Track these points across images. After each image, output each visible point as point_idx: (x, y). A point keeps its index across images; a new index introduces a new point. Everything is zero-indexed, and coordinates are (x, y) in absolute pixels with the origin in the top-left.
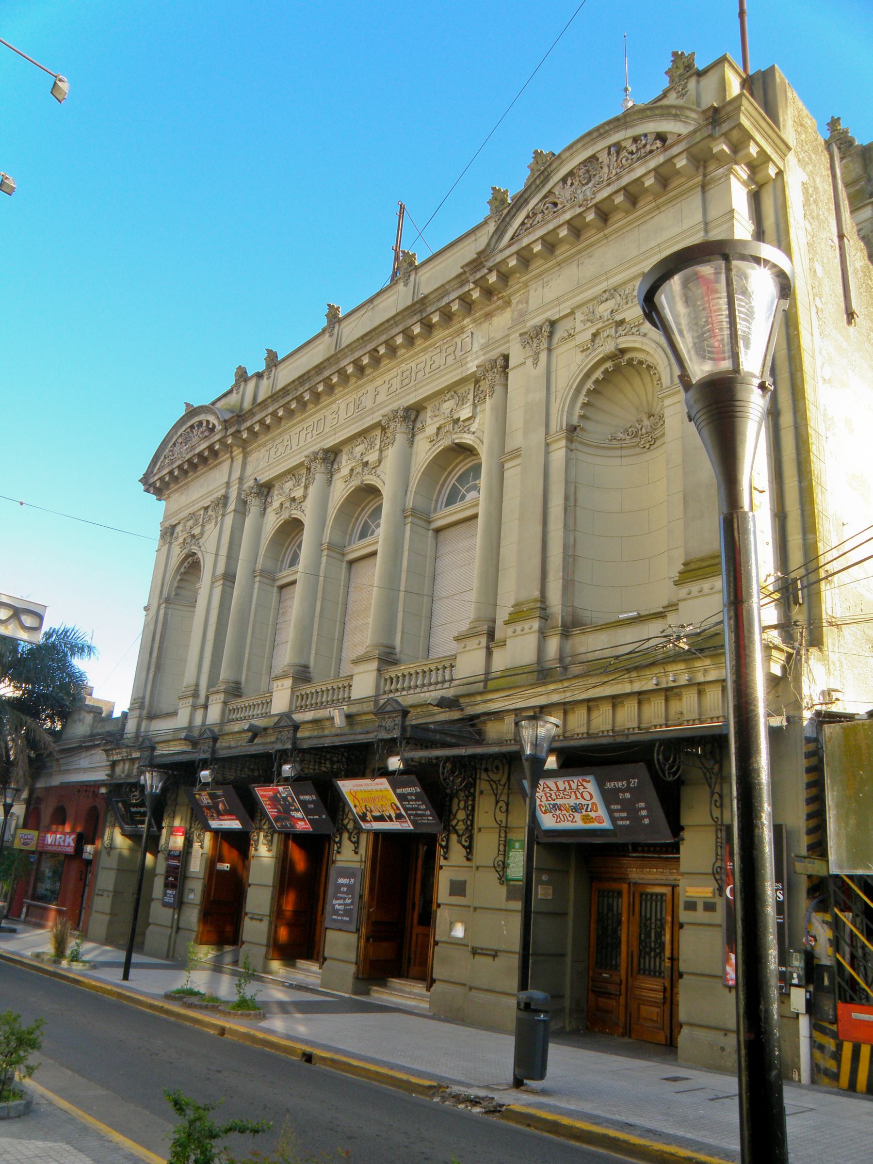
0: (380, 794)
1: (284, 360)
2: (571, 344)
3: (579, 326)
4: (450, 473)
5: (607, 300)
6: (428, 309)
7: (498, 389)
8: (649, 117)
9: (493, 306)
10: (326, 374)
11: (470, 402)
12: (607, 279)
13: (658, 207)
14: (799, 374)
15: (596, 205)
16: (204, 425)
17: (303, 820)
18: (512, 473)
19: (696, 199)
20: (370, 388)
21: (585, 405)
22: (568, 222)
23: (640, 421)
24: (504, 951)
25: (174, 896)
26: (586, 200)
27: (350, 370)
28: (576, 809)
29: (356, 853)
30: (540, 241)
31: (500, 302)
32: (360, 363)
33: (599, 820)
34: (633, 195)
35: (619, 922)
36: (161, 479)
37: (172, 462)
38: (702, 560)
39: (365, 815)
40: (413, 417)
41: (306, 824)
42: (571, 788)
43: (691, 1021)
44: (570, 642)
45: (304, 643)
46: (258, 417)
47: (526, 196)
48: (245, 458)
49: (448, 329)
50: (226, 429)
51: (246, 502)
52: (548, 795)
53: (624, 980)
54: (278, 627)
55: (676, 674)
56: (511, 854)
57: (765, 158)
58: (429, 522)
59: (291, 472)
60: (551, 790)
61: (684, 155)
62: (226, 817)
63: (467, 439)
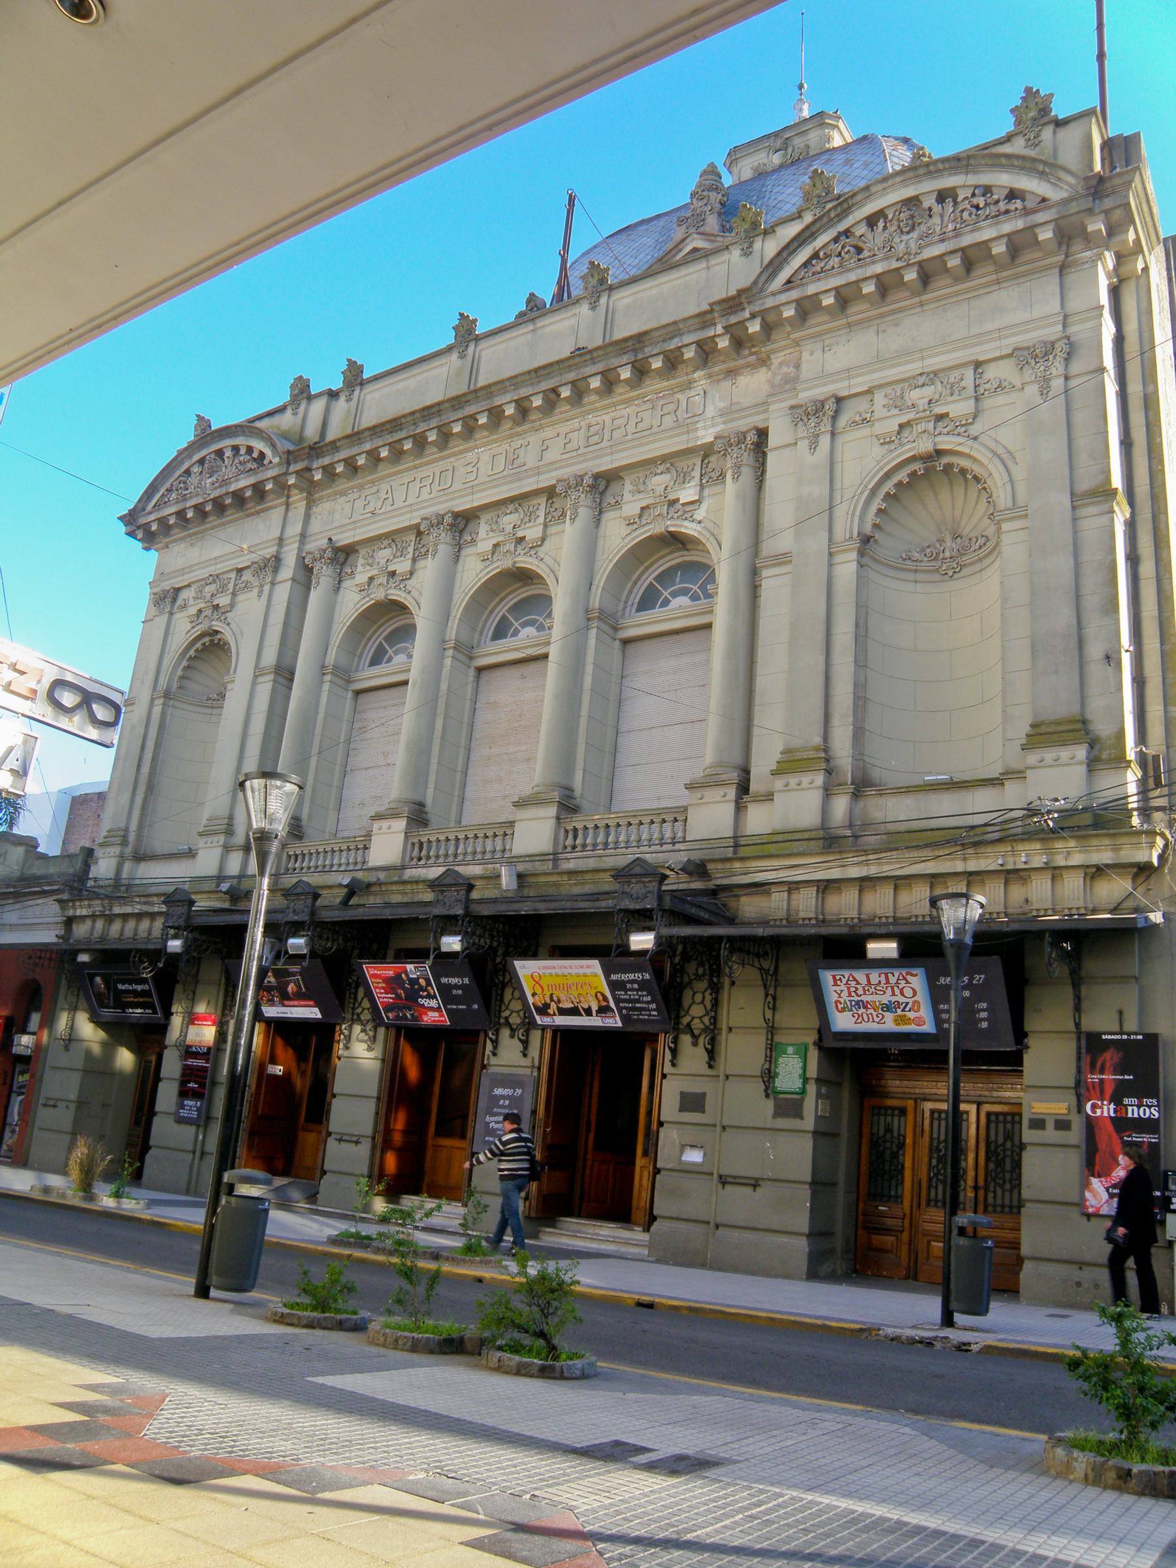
0: (582, 980)
2: (866, 431)
3: (879, 412)
4: (647, 568)
5: (923, 385)
6: (646, 350)
7: (747, 474)
8: (1001, 165)
9: (742, 362)
10: (470, 410)
11: (696, 481)
12: (922, 358)
13: (998, 282)
14: (1162, 517)
15: (920, 263)
16: (243, 451)
17: (438, 1009)
18: (773, 584)
19: (1051, 284)
20: (534, 439)
21: (880, 511)
22: (878, 277)
23: (941, 541)
24: (769, 1180)
25: (199, 1110)
26: (909, 254)
27: (510, 410)
28: (888, 1008)
29: (525, 1055)
30: (833, 293)
31: (753, 358)
32: (526, 403)
33: (919, 1021)
34: (972, 259)
35: (902, 1145)
36: (162, 521)
37: (185, 498)
38: (1058, 723)
39: (547, 1006)
40: (602, 488)
41: (155, 1012)
42: (887, 981)
43: (1038, 1255)
44: (861, 804)
45: (418, 771)
46: (343, 454)
47: (814, 229)
48: (309, 508)
49: (668, 380)
50: (289, 464)
51: (310, 570)
52: (852, 989)
53: (908, 1213)
54: (352, 746)
55: (1030, 855)
56: (781, 1060)
57: (1138, 249)
58: (616, 629)
59: (391, 537)
60: (858, 983)
61: (1051, 226)
62: (296, 1003)
63: (689, 528)
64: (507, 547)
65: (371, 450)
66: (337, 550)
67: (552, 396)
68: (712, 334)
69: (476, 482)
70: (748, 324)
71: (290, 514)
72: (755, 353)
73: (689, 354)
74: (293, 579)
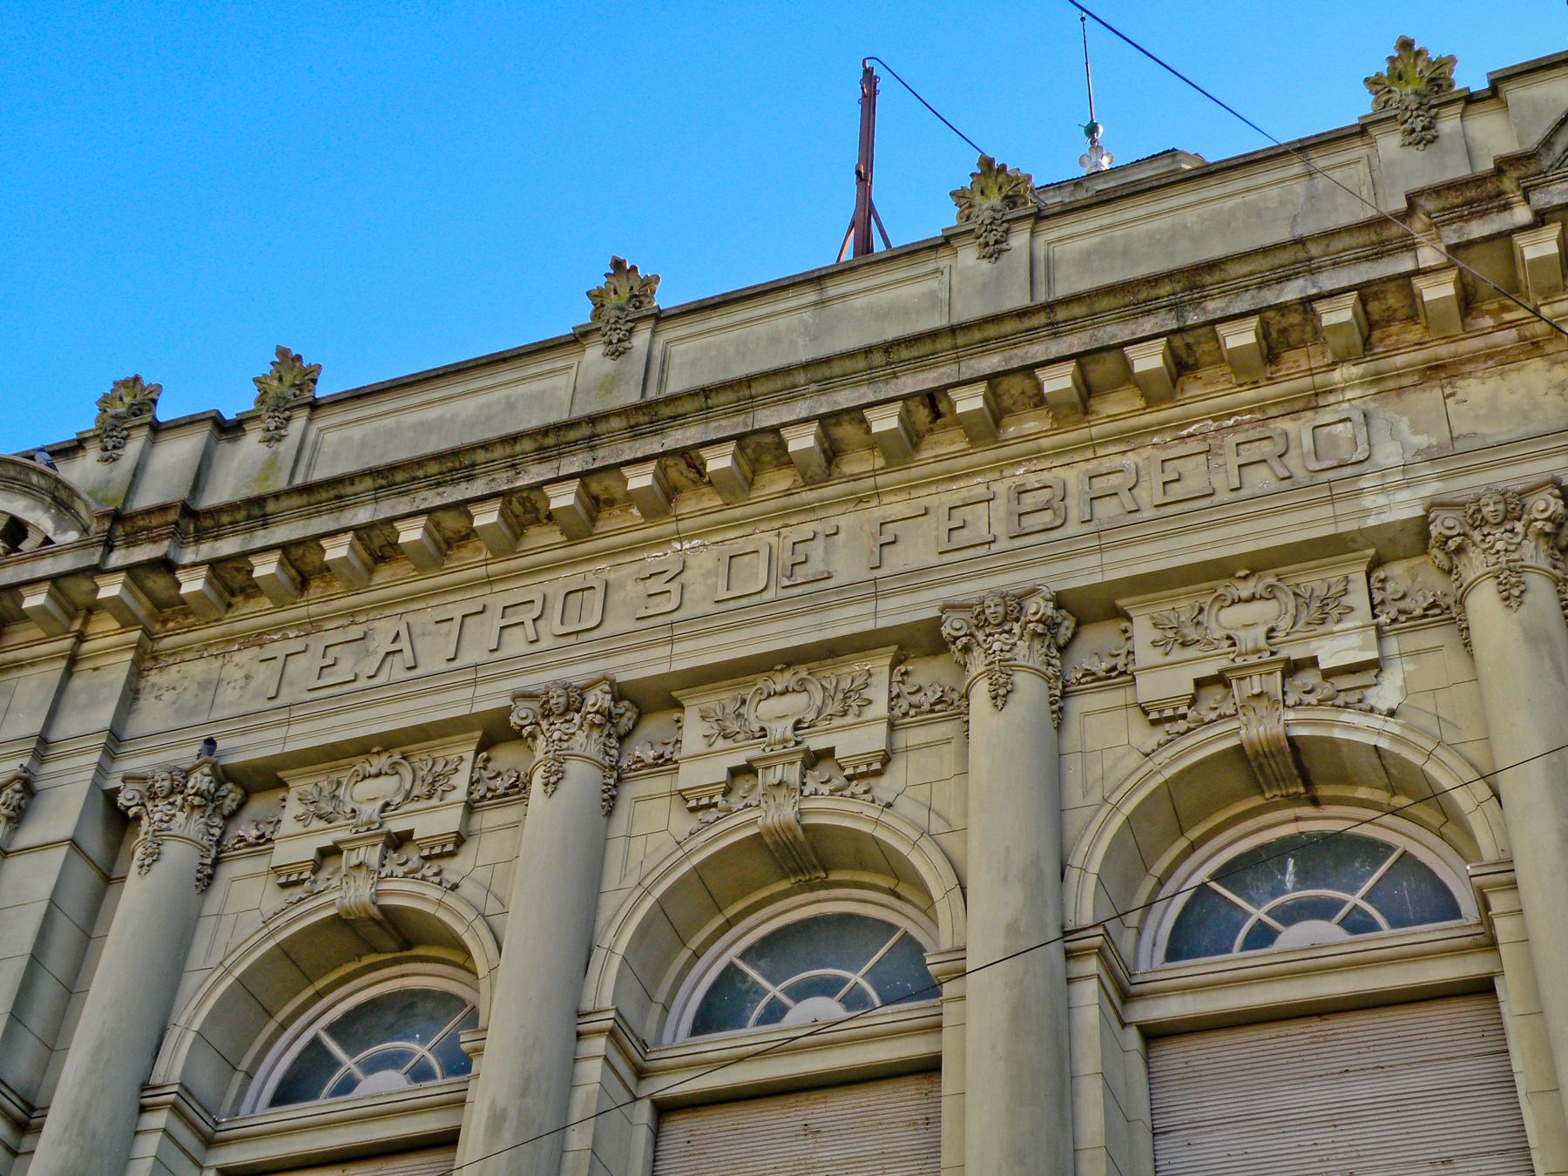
1: (338, 401)
4: (1193, 847)
48: (138, 671)
49: (1255, 384)
50: (109, 546)
64: (776, 774)
65: (370, 526)
66: (224, 775)
67: (922, 414)
68: (1404, 264)
69: (676, 616)
70: (1520, 240)
71: (77, 683)
72: (1512, 324)
73: (1337, 314)
74: (73, 843)
